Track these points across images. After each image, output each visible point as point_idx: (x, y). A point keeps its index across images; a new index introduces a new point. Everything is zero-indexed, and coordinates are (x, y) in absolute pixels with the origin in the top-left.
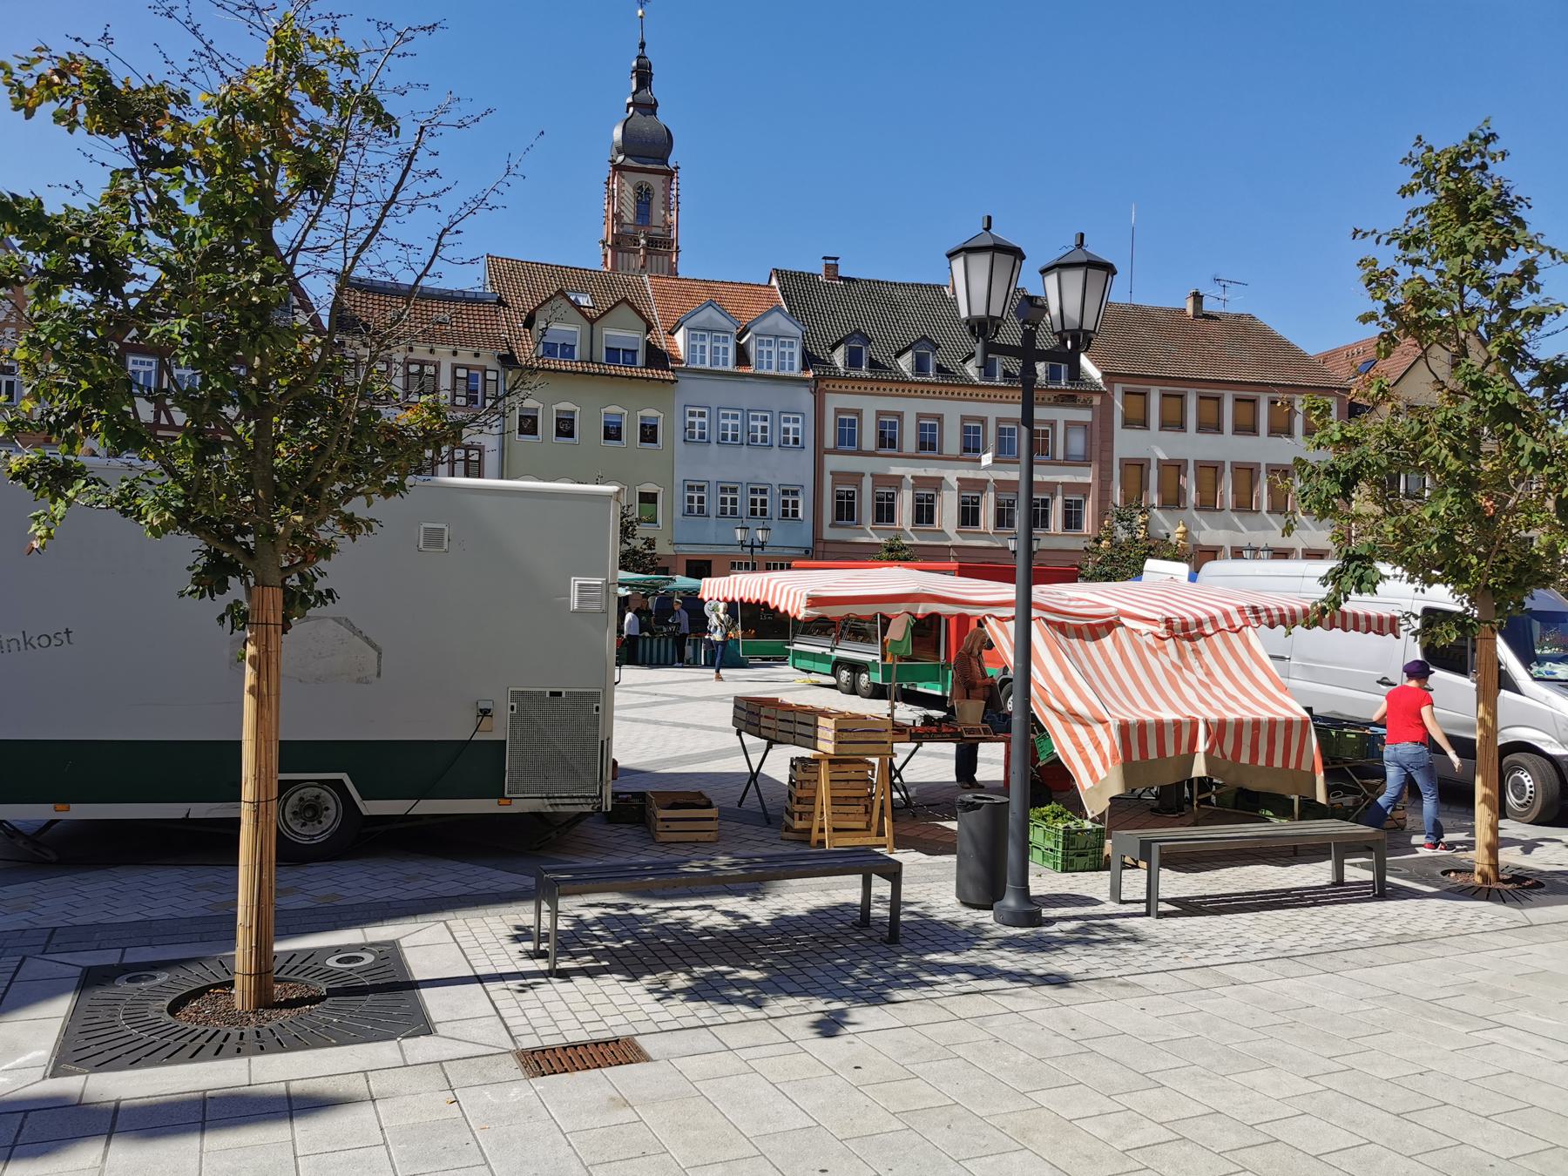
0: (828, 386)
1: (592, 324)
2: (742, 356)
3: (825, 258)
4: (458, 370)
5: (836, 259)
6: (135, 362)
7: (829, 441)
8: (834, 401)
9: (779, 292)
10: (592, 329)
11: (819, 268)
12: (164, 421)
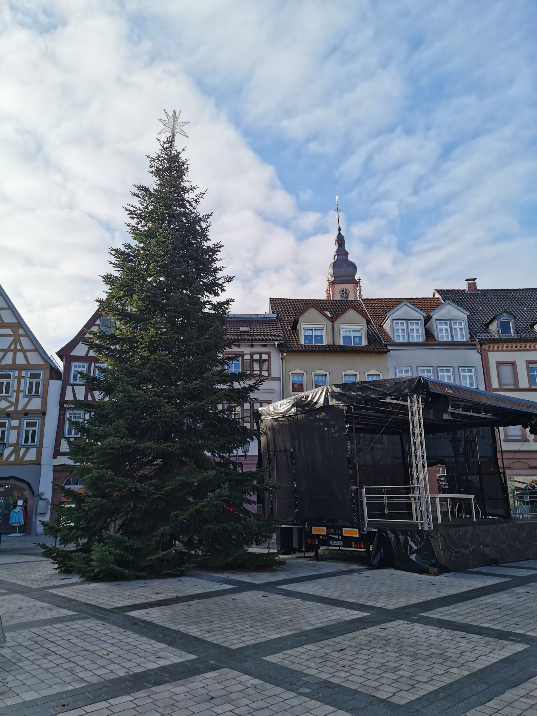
0: (489, 347)
1: (333, 322)
2: (429, 334)
3: (467, 280)
4: (254, 355)
5: (475, 279)
6: (75, 366)
7: (495, 384)
8: (494, 357)
9: (442, 300)
10: (333, 325)
11: (464, 286)
12: (90, 398)
